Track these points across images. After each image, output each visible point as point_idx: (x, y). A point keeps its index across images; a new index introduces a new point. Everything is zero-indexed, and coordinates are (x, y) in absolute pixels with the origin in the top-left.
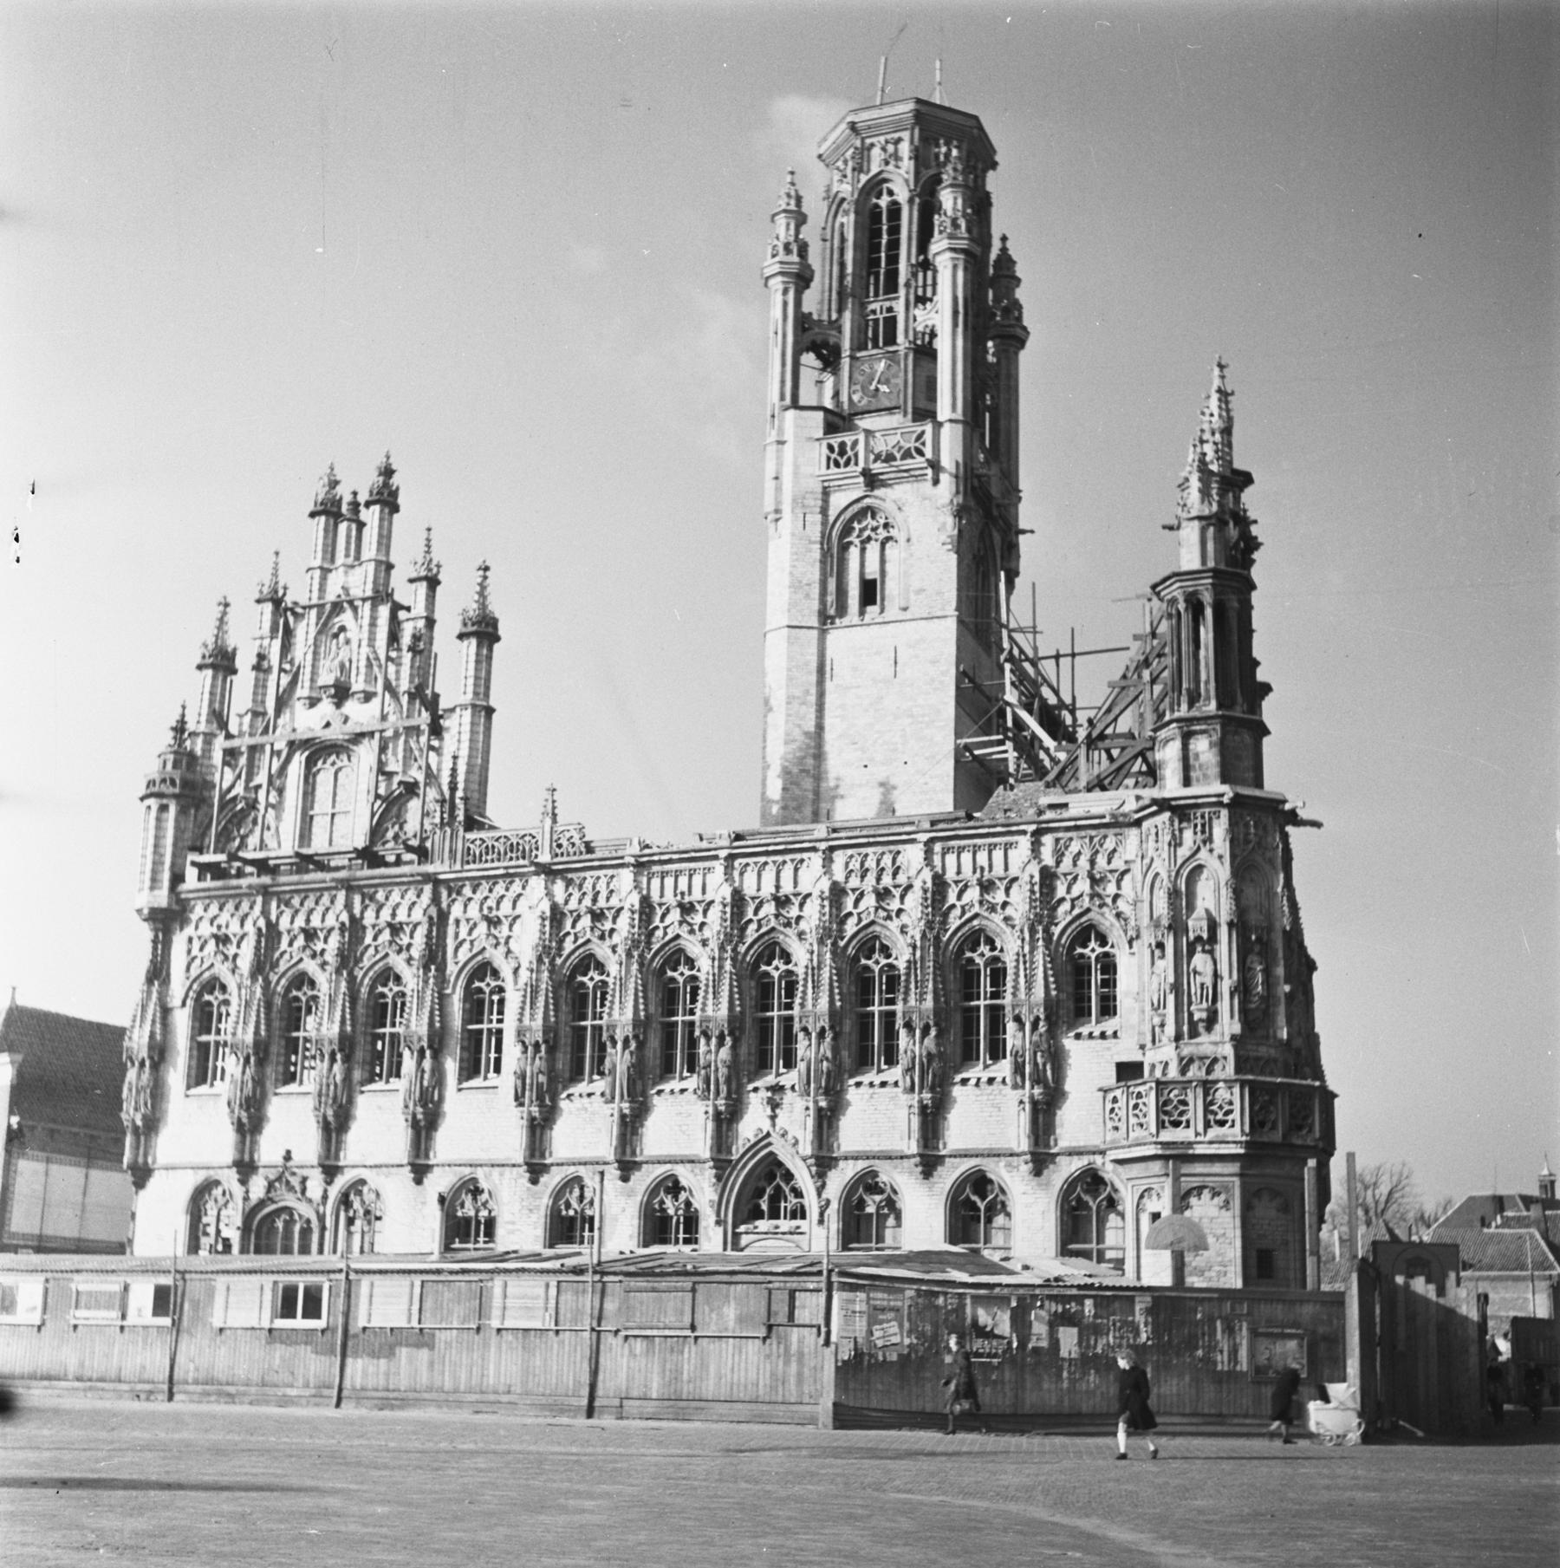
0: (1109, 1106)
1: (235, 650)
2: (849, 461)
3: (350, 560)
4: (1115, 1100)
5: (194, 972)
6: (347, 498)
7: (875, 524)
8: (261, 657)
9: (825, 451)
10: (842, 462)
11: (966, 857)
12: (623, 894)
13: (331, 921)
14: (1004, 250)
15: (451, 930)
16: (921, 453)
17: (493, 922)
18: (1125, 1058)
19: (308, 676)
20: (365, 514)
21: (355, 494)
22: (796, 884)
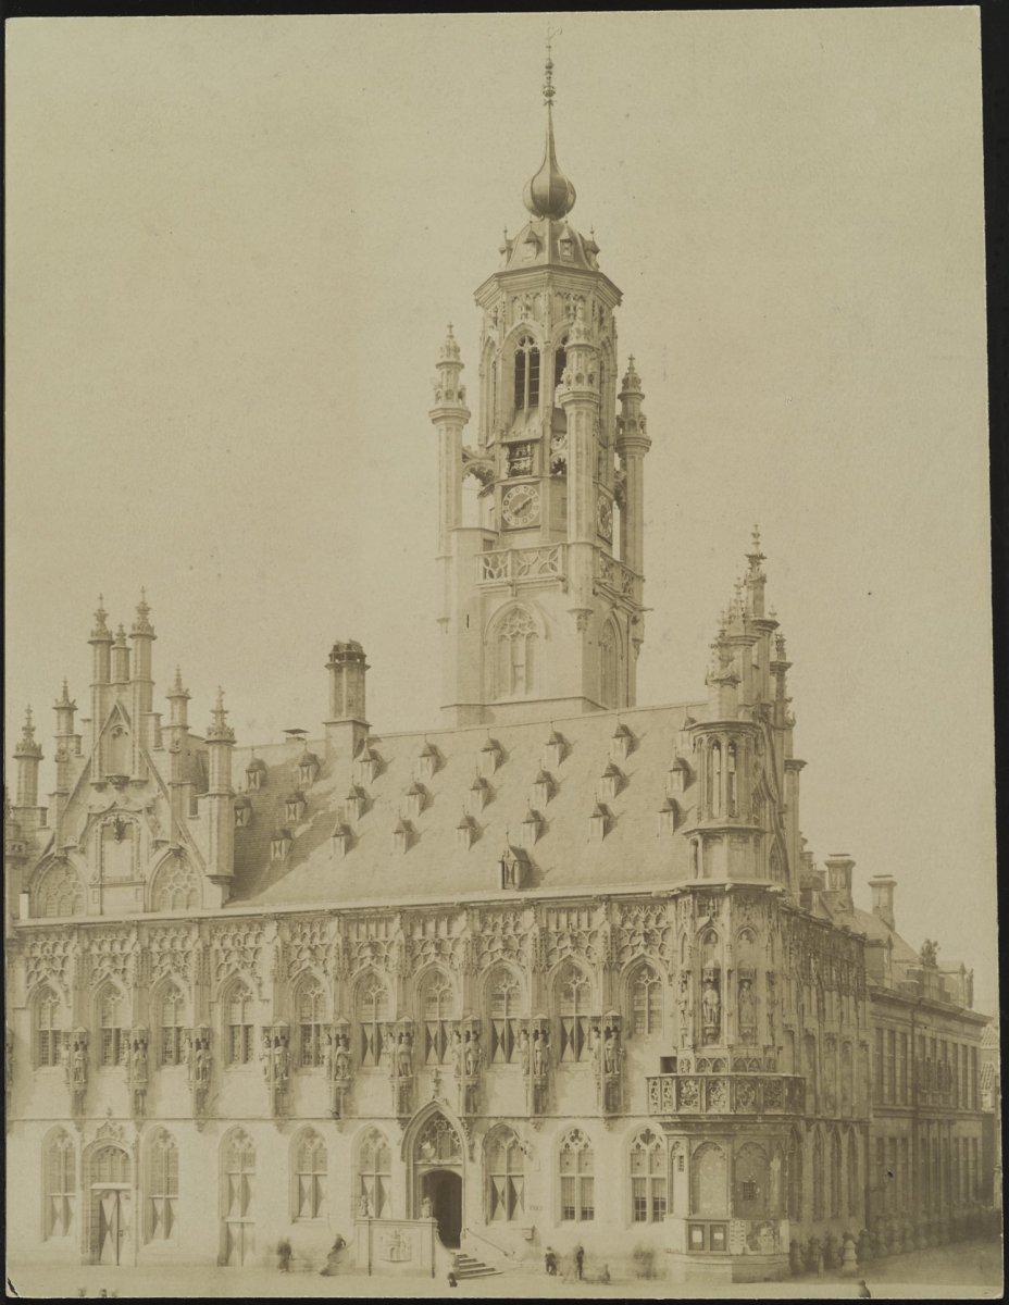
0: (651, 1087)
1: (40, 746)
2: (500, 572)
3: (121, 680)
4: (655, 1084)
5: (33, 982)
6: (116, 630)
7: (522, 621)
8: (62, 752)
9: (482, 564)
10: (495, 573)
11: (563, 918)
12: (332, 936)
13: (127, 949)
14: (631, 368)
15: (213, 958)
16: (553, 567)
17: (243, 952)
18: (667, 1054)
19: (97, 767)
20: (130, 643)
21: (121, 626)
22: (449, 932)
